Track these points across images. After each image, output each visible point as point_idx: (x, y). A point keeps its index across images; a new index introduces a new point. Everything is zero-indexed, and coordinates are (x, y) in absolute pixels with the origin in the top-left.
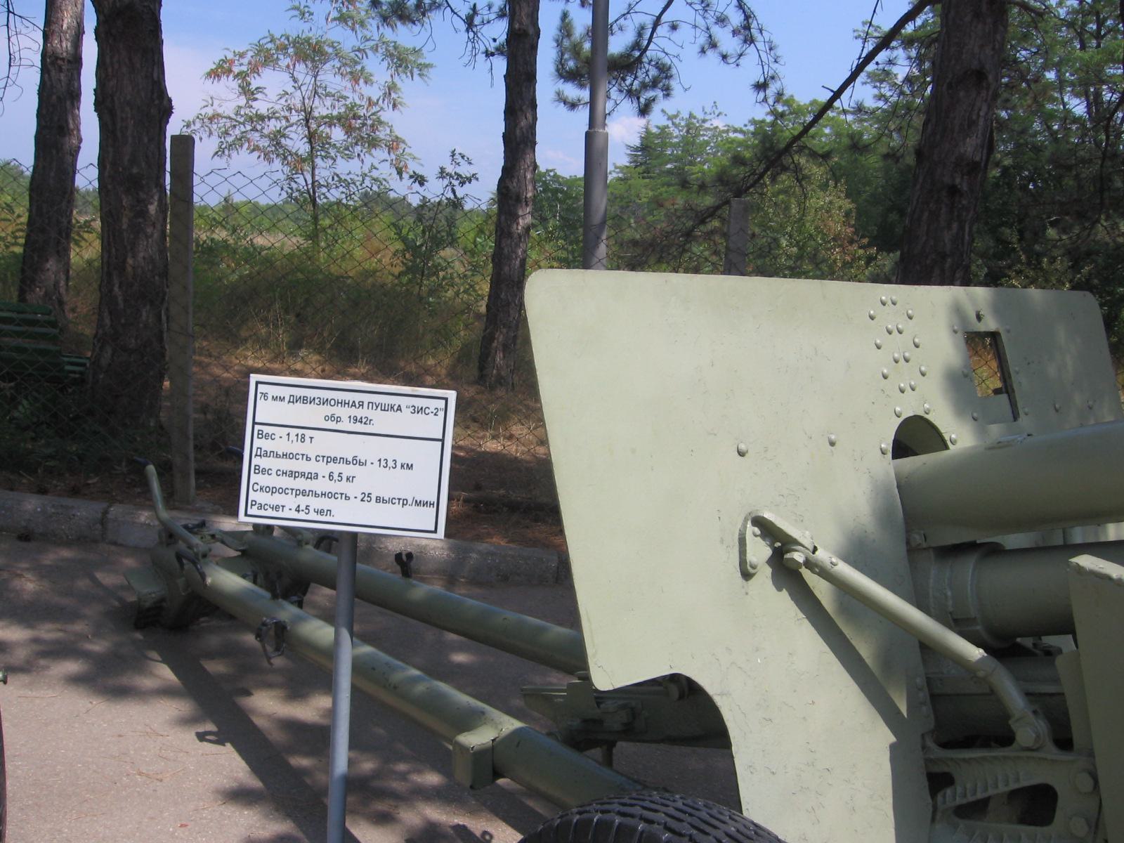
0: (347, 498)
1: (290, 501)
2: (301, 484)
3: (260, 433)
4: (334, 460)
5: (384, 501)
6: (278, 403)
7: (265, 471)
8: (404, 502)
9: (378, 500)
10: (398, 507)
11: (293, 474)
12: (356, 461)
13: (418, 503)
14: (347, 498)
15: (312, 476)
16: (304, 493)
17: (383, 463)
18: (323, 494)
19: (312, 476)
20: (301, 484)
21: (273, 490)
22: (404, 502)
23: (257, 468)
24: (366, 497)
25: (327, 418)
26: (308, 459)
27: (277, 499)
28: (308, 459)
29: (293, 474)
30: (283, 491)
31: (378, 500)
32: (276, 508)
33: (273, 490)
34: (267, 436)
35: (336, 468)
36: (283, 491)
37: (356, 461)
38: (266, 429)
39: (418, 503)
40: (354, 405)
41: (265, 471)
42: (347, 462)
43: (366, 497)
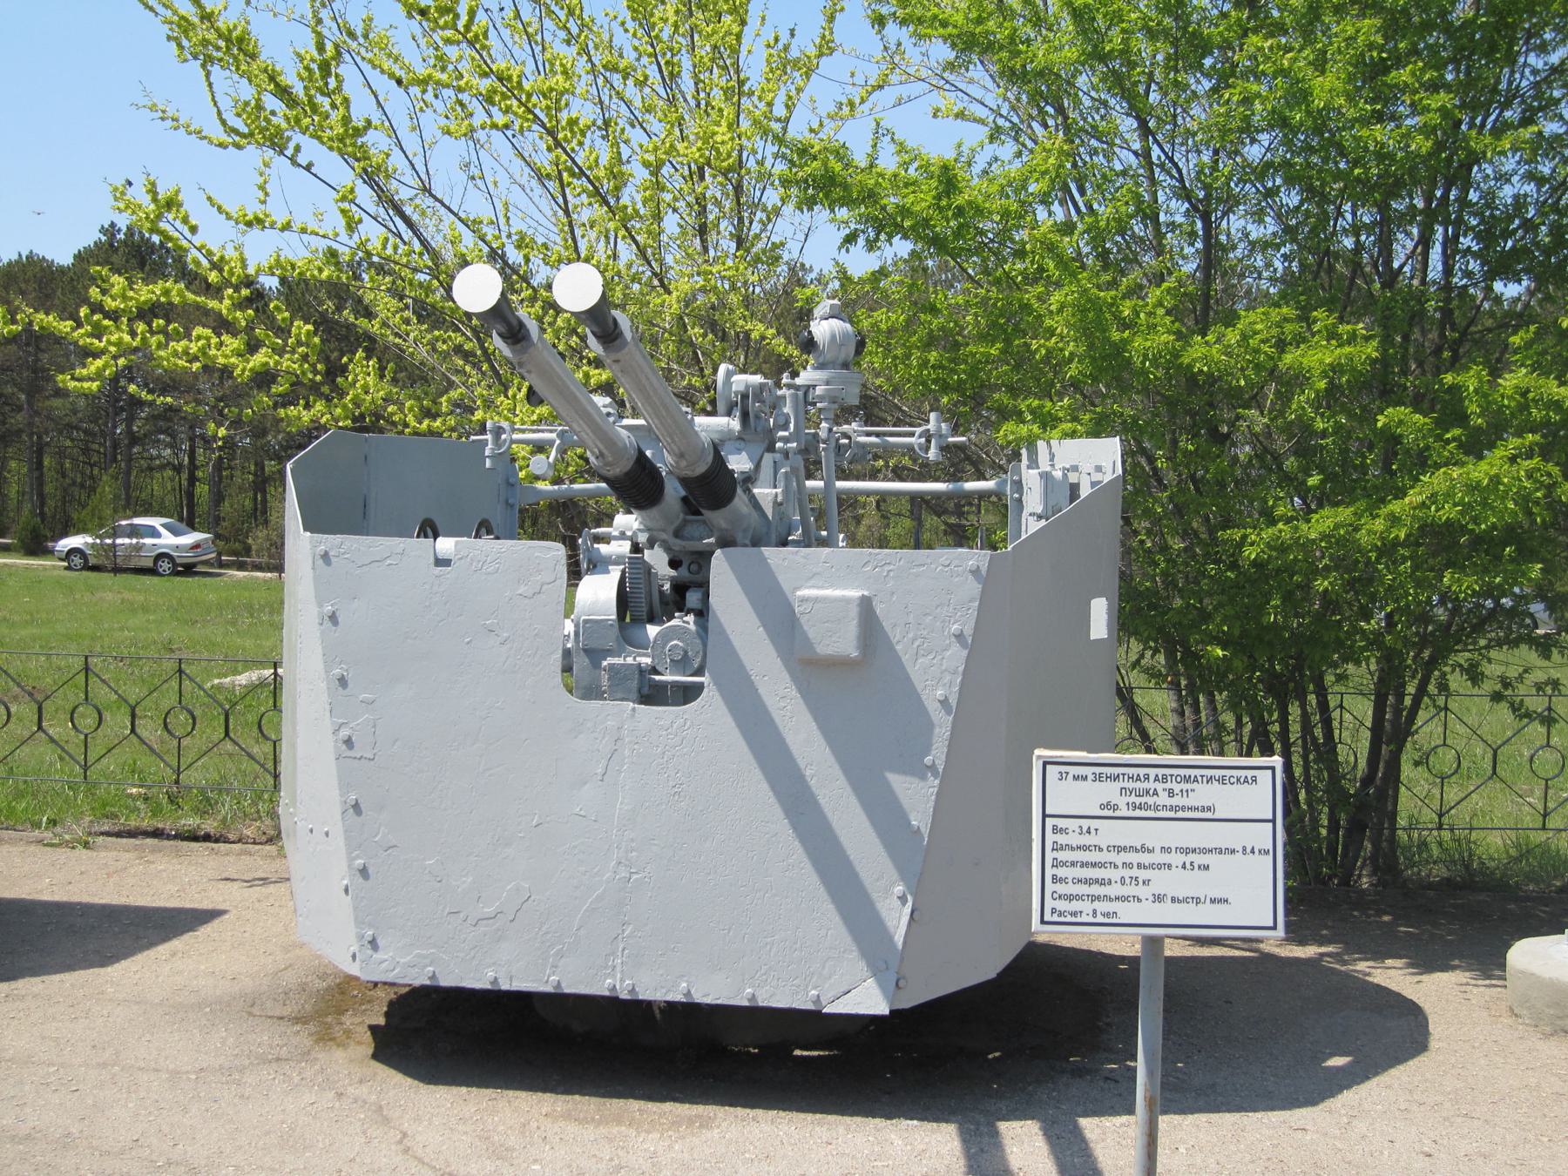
0: (1139, 900)
2: (1096, 890)
3: (1055, 829)
5: (1179, 901)
6: (1080, 783)
9: (1173, 900)
13: (1213, 901)
14: (1139, 900)
16: (1098, 898)
18: (1117, 898)
21: (1070, 898)
22: (1198, 901)
24: (1158, 898)
30: (1078, 897)
31: (1173, 900)
33: (1070, 898)
34: (1063, 831)
36: (1078, 897)
38: (1061, 823)
39: (1213, 901)
40: (1139, 779)
43: (1158, 898)
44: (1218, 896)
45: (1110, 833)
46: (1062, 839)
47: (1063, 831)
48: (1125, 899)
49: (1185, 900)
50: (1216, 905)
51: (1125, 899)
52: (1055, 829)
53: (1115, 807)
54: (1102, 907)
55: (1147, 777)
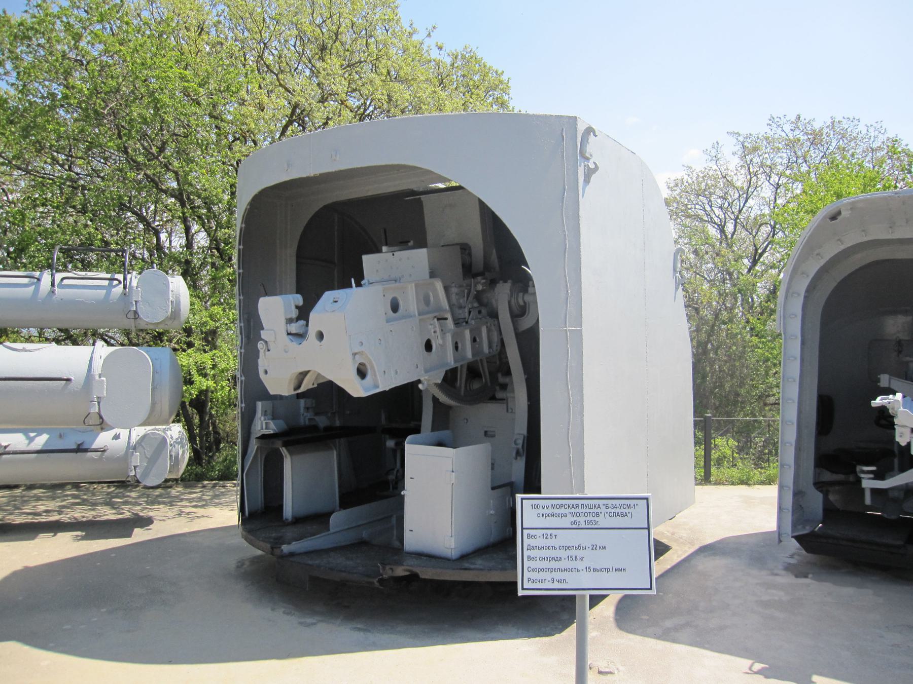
0: (578, 571)
1: (547, 576)
2: (553, 564)
3: (529, 536)
4: (569, 548)
7: (534, 559)
8: (608, 570)
9: (594, 570)
10: (605, 573)
11: (548, 559)
12: (580, 547)
14: (578, 571)
15: (559, 559)
17: (594, 547)
19: (559, 559)
20: (553, 564)
21: (538, 570)
22: (608, 570)
23: (529, 557)
24: (588, 569)
25: (572, 523)
26: (555, 549)
27: (541, 575)
28: (555, 549)
29: (548, 559)
30: (544, 570)
31: (594, 570)
32: (541, 581)
33: (538, 570)
34: (534, 537)
35: (573, 553)
36: (544, 570)
37: (580, 547)
38: (532, 532)
41: (534, 559)
42: (576, 548)
44: (620, 567)
45: (565, 538)
46: (532, 542)
47: (534, 537)
48: (570, 570)
49: (601, 570)
50: (619, 572)
51: (570, 570)
52: (529, 536)
53: (579, 523)
54: (557, 575)
55: (577, 506)
